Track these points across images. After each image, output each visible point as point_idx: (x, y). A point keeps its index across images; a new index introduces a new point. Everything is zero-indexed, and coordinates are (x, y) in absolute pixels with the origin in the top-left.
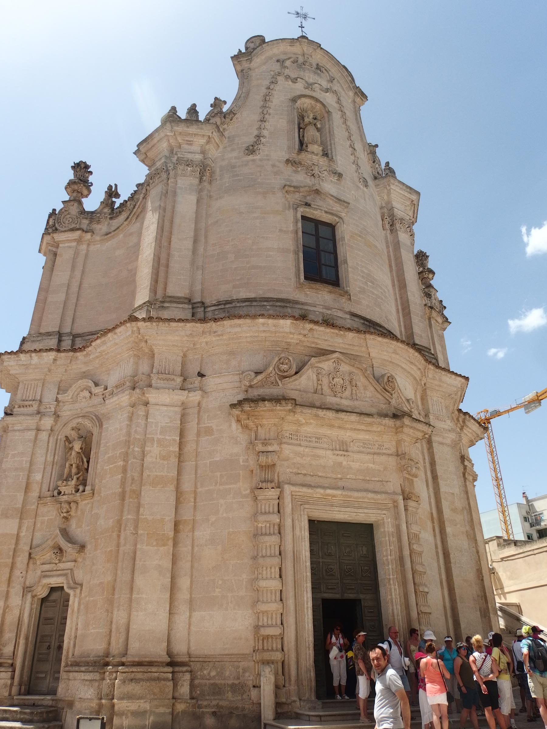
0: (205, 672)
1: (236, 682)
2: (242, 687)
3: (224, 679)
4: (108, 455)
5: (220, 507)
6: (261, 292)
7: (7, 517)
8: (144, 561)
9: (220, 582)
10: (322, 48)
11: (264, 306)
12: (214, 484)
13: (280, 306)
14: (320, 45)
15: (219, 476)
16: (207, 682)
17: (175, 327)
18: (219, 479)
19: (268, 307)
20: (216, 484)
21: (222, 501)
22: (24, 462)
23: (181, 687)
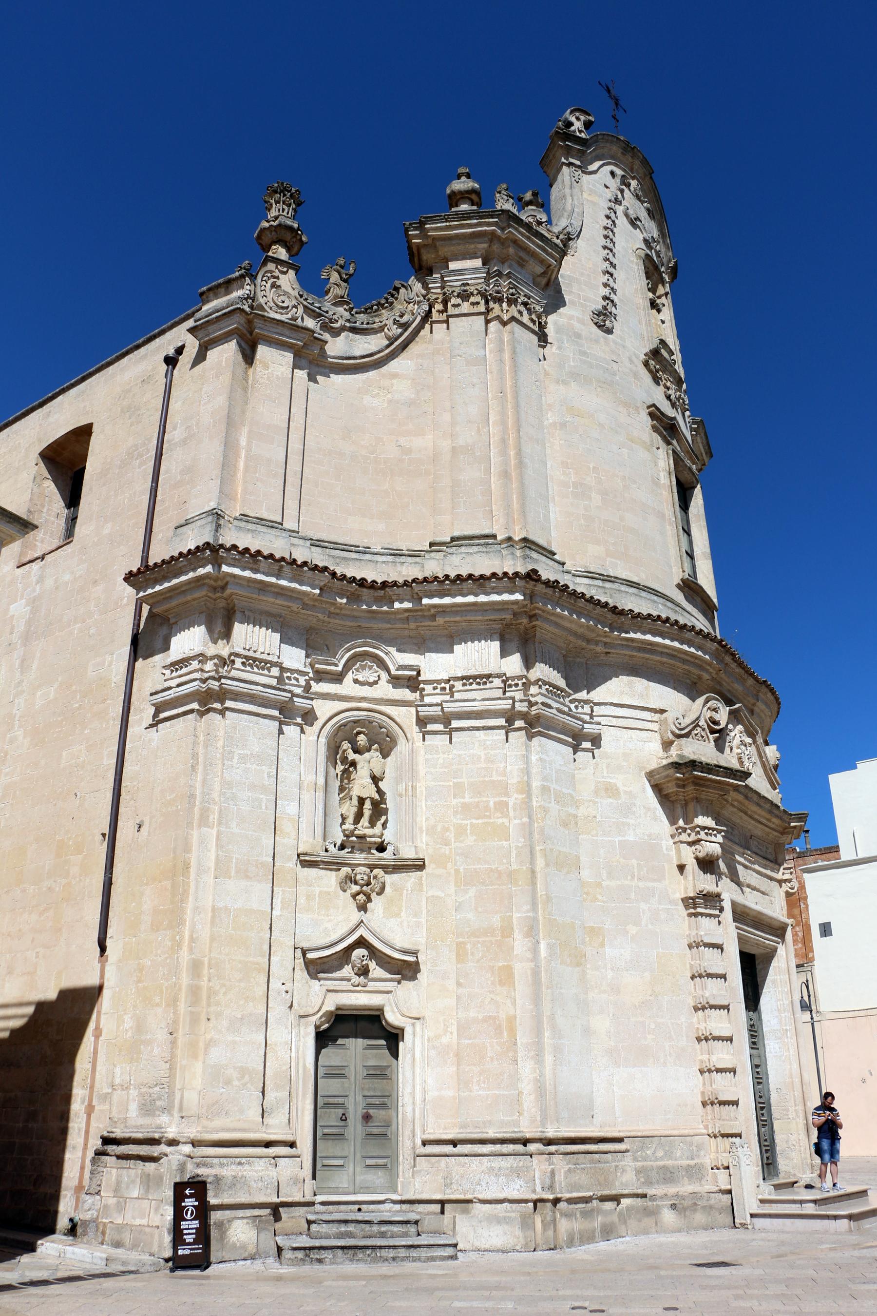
0: (648, 1152)
1: (692, 1163)
2: (700, 1170)
3: (676, 1160)
4: (462, 800)
5: (641, 914)
6: (643, 576)
7: (247, 877)
8: (561, 988)
9: (653, 1026)
10: (651, 178)
11: (655, 602)
12: (629, 878)
13: (672, 609)
14: (653, 172)
15: (636, 866)
16: (655, 1164)
17: (580, 607)
18: (636, 870)
19: (660, 605)
20: (633, 877)
21: (643, 906)
22: (266, 776)
23: (622, 1173)
